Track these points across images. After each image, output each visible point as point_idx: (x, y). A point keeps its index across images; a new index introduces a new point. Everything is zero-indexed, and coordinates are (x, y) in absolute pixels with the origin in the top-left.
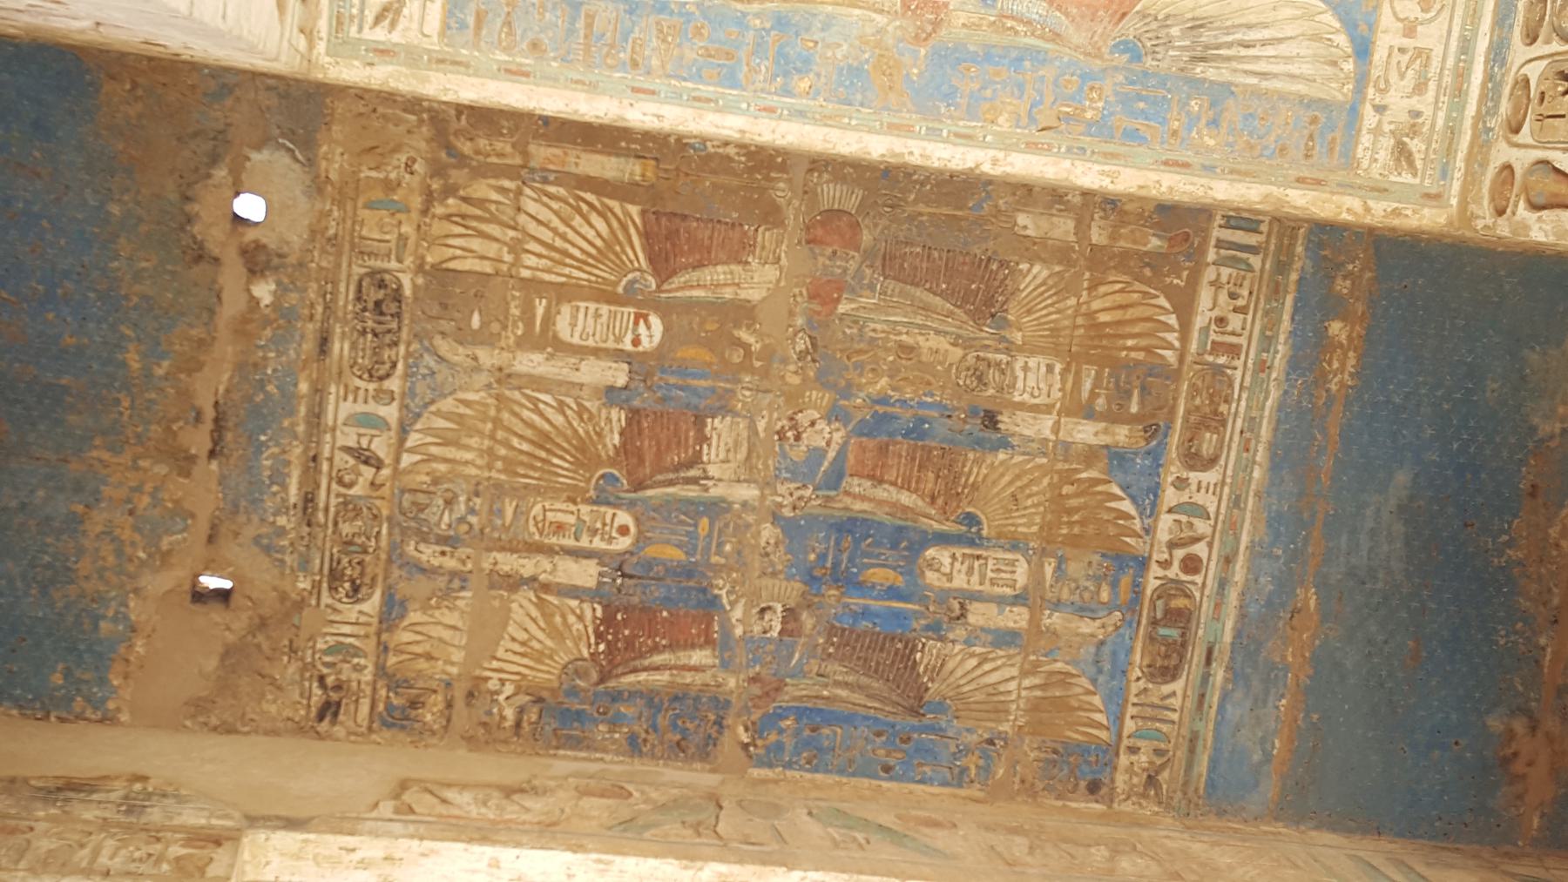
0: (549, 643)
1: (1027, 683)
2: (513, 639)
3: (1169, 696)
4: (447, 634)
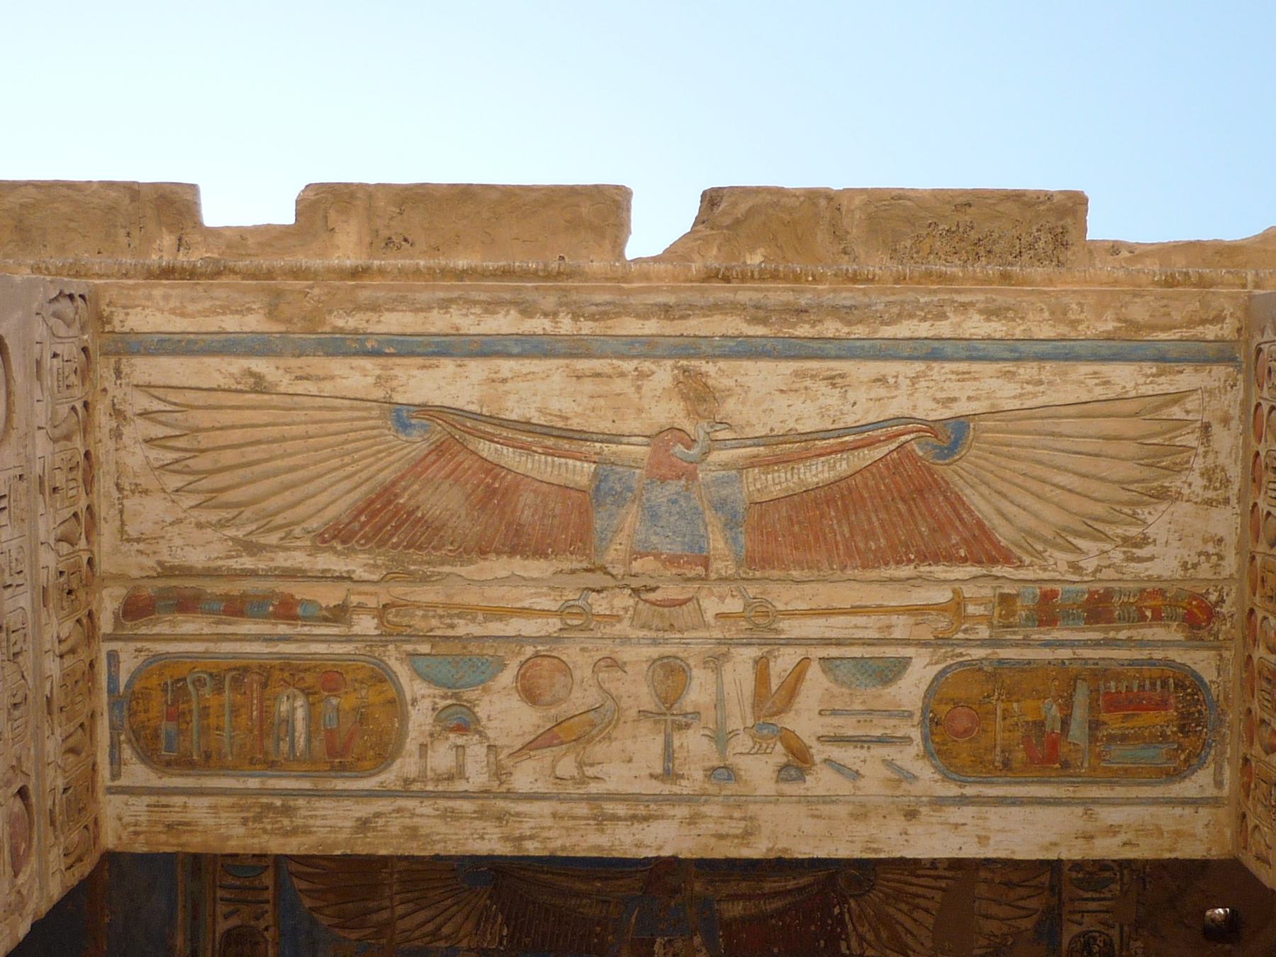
0: (891, 910)
1: (385, 915)
2: (927, 911)
3: (231, 914)
4: (994, 910)
